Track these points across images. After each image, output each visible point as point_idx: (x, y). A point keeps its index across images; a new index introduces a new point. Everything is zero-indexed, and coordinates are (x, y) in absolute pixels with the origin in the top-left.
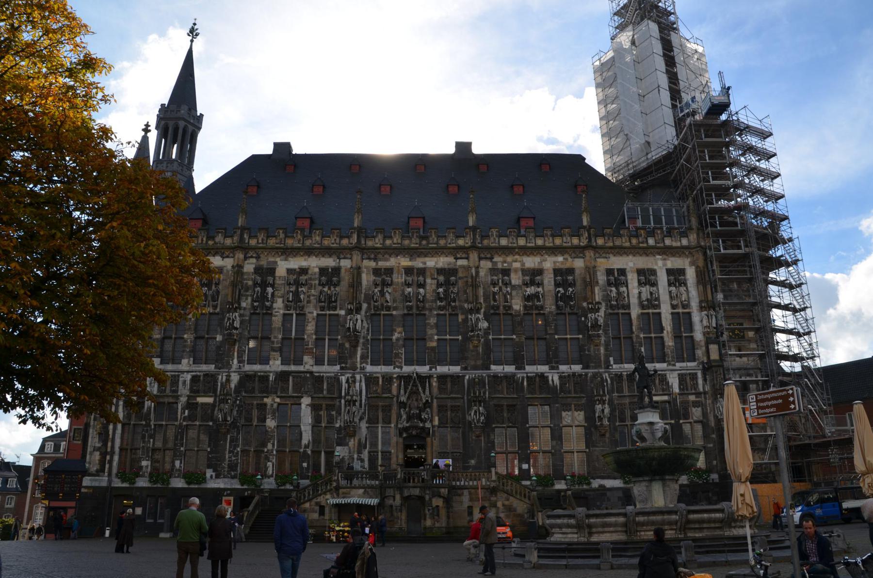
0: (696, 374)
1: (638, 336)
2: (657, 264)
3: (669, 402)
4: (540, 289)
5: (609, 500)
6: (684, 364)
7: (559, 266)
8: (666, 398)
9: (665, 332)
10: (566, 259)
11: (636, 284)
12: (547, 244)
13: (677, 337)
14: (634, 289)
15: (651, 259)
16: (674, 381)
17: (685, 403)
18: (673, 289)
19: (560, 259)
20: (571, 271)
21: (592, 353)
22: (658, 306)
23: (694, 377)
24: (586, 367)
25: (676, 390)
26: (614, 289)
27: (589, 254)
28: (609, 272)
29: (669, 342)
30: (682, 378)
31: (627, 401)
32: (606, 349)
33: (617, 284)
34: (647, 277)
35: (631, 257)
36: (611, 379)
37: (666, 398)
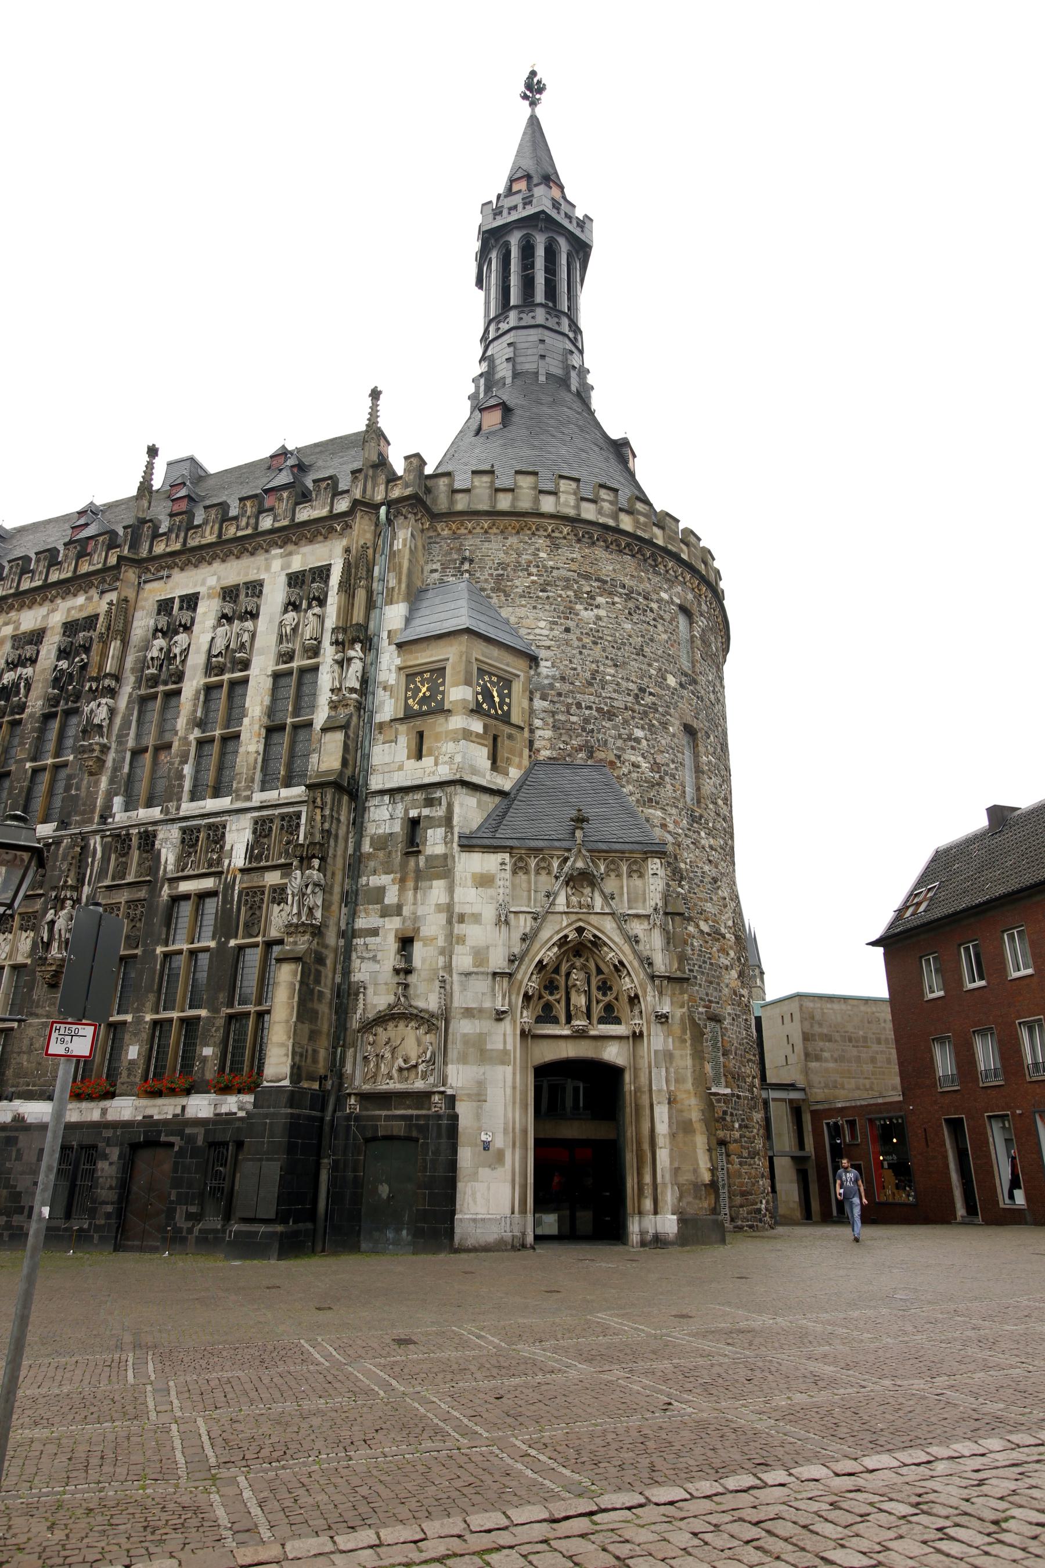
0: (298, 815)
1: (185, 740)
2: (268, 568)
3: (212, 894)
4: (28, 671)
5: (19, 1157)
6: (271, 796)
7: (76, 615)
8: (208, 883)
9: (246, 721)
10: (89, 599)
11: (211, 621)
12: (63, 576)
13: (273, 730)
14: (205, 633)
15: (260, 559)
16: (239, 838)
17: (254, 893)
18: (291, 615)
19: (81, 600)
20: (91, 621)
21: (83, 793)
22: (246, 665)
23: (291, 822)
24: (63, 825)
25: (239, 860)
26: (160, 642)
27: (130, 575)
28: (164, 606)
29: (251, 743)
30: (261, 829)
31: (123, 897)
32: (112, 781)
33: (168, 632)
34: (240, 603)
35: (217, 565)
36: (104, 847)
37: (208, 883)
